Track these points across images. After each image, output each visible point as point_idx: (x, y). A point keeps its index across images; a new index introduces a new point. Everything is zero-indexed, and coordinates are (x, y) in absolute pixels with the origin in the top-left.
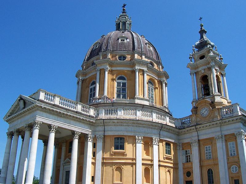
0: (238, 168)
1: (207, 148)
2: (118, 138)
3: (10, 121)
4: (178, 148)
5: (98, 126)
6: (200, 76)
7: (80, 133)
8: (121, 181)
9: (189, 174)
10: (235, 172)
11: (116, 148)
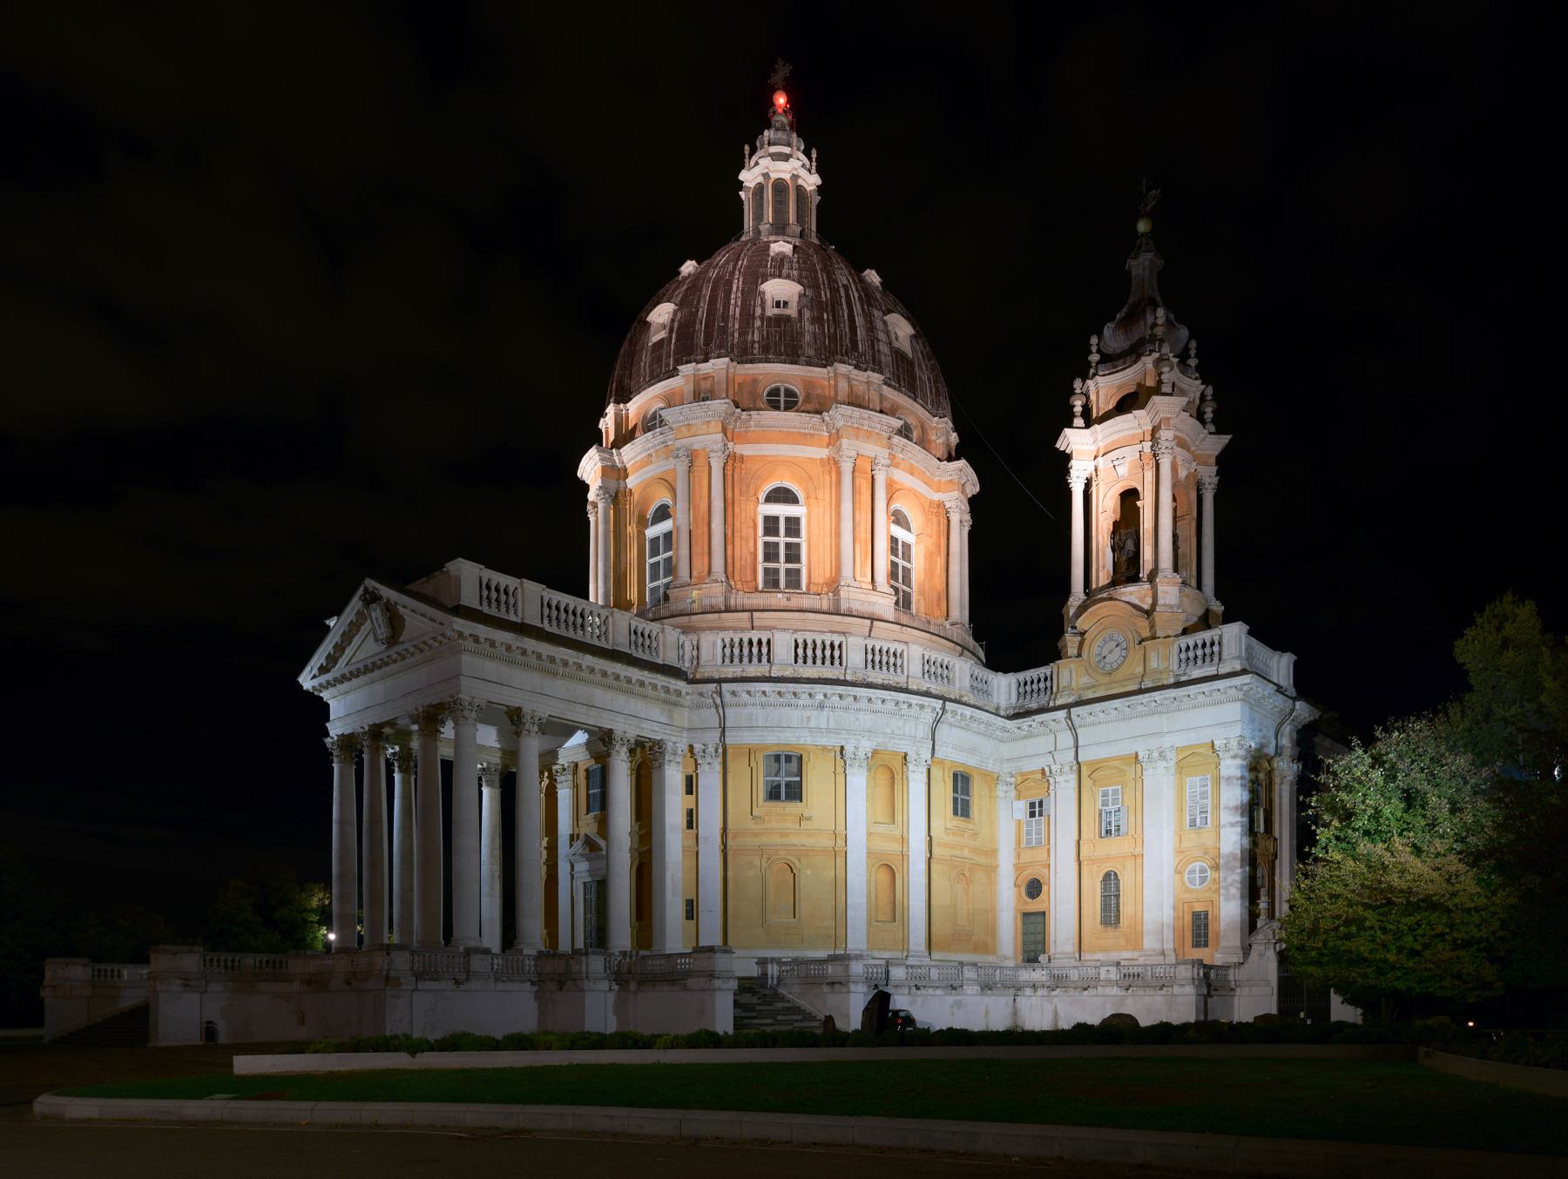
1: (1105, 794)
2: (777, 758)
4: (1001, 794)
7: (633, 741)
9: (1034, 888)
10: (1197, 887)
11: (773, 794)
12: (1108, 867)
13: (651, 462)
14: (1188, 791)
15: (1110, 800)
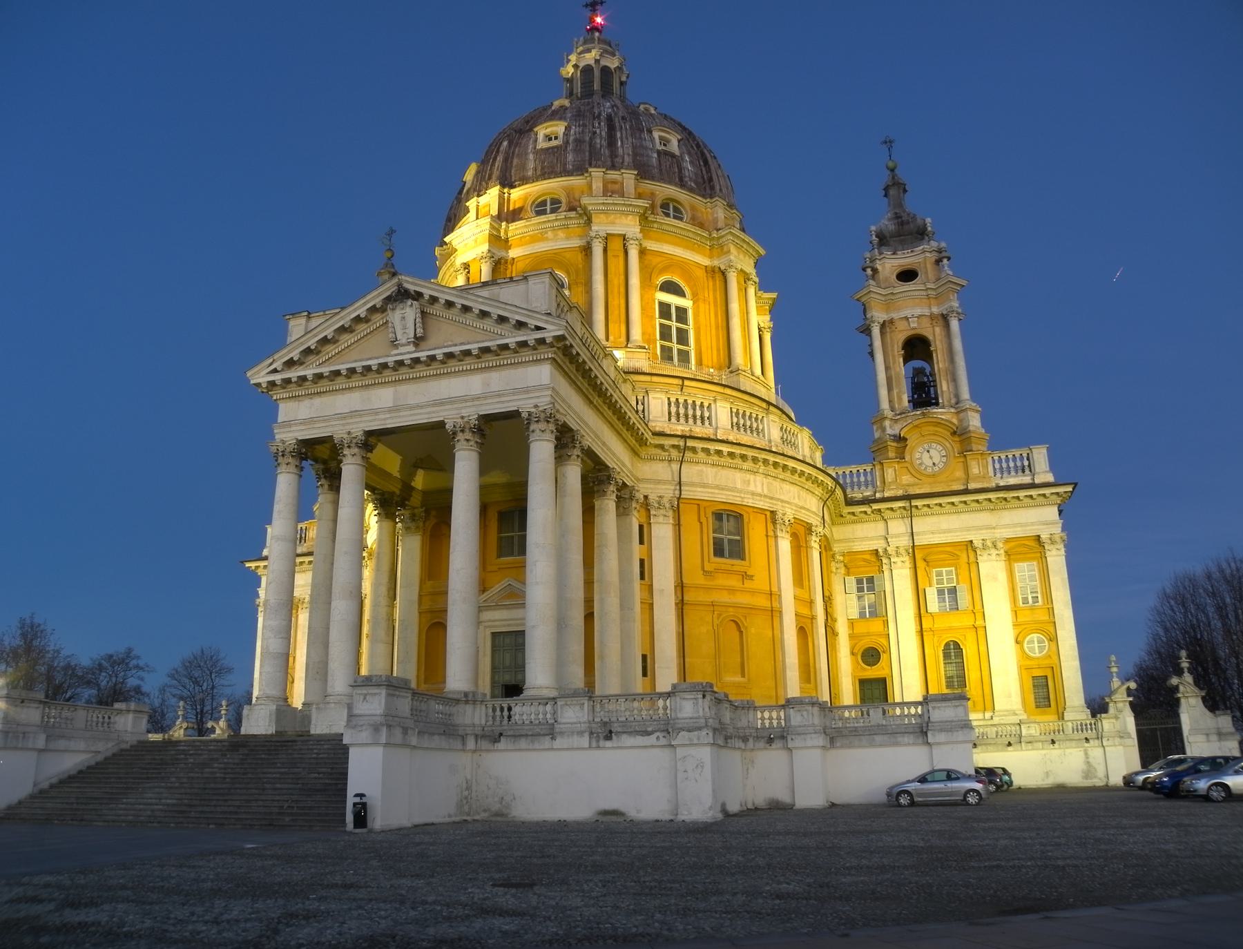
0: (1047, 643)
2: (718, 516)
6: (900, 337)
8: (743, 676)
9: (871, 656)
10: (1038, 655)
11: (719, 551)
12: (948, 637)
13: (547, 239)
14: (1017, 574)
15: (945, 581)
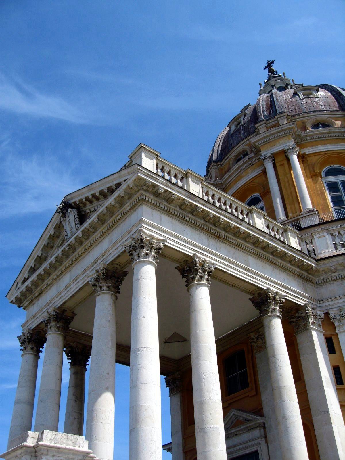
3: (31, 298)
5: (326, 282)
